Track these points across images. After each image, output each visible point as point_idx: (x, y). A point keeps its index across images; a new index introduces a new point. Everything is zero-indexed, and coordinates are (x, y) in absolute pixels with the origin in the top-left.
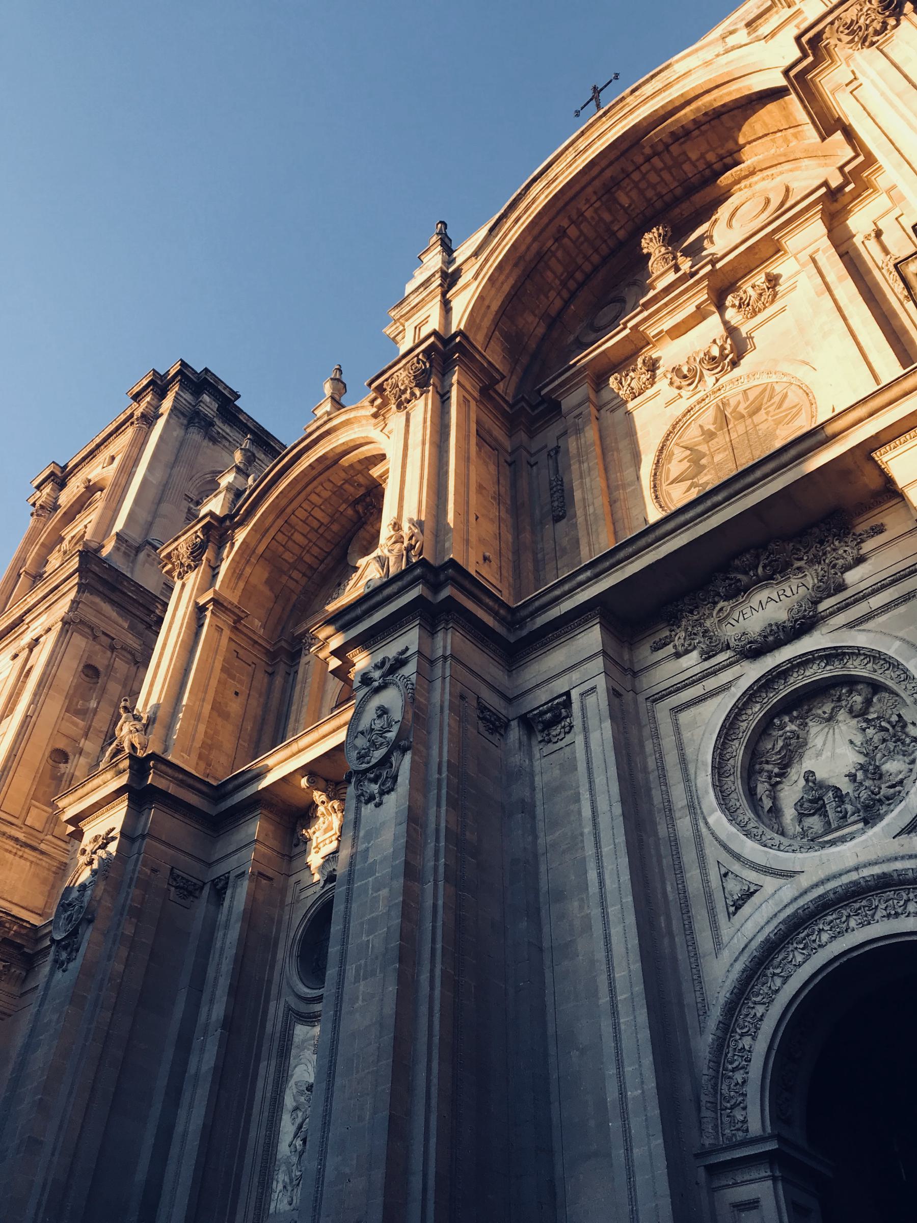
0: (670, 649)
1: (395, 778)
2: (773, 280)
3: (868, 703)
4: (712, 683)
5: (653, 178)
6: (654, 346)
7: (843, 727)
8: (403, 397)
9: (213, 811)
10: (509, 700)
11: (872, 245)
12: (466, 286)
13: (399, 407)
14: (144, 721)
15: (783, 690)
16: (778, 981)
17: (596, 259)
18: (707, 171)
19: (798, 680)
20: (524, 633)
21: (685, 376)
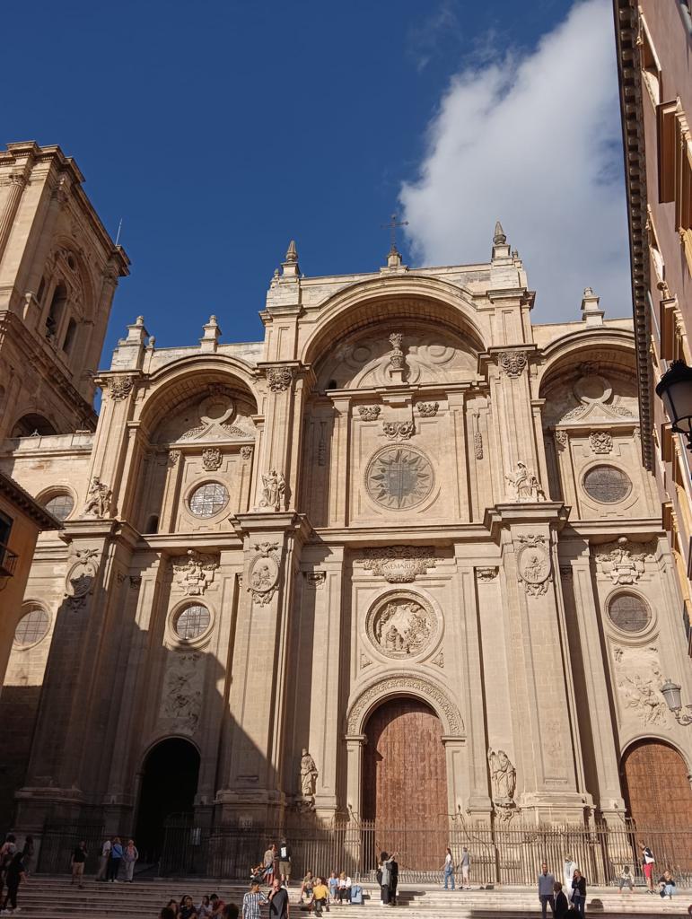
0: (362, 565)
1: (271, 600)
2: (437, 406)
3: (417, 610)
4: (373, 584)
5: (406, 307)
6: (382, 403)
7: (407, 613)
8: (276, 385)
9: (135, 545)
10: (300, 563)
11: (475, 419)
12: (310, 322)
13: (272, 388)
14: (106, 492)
15: (395, 596)
16: (373, 694)
17: (366, 322)
18: (428, 317)
19: (400, 595)
20: (314, 540)
21: (389, 430)
